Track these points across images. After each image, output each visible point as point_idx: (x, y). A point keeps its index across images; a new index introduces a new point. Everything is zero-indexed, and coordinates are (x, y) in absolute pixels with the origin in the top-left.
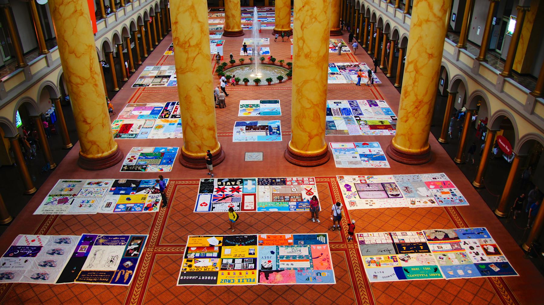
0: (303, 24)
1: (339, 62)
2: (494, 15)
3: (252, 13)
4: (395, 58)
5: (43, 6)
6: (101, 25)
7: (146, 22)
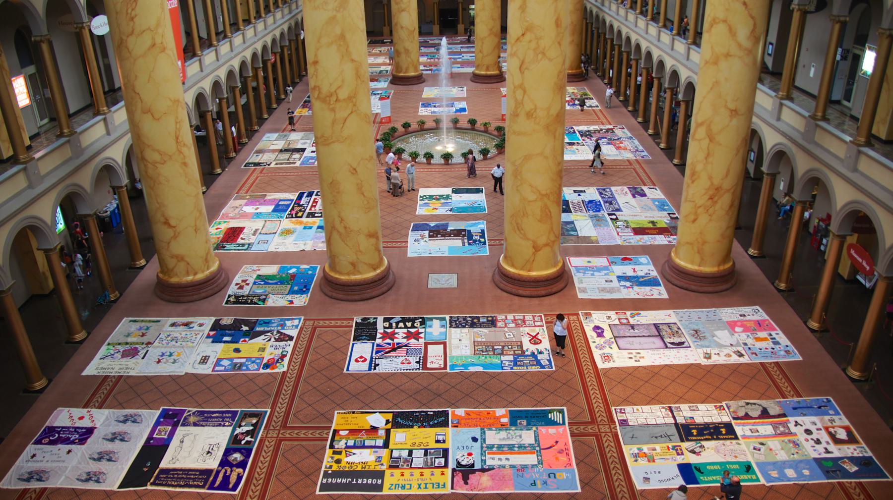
0: (523, 62)
3: (437, 46)
5: (102, 38)
6: (193, 68)
7: (265, 62)
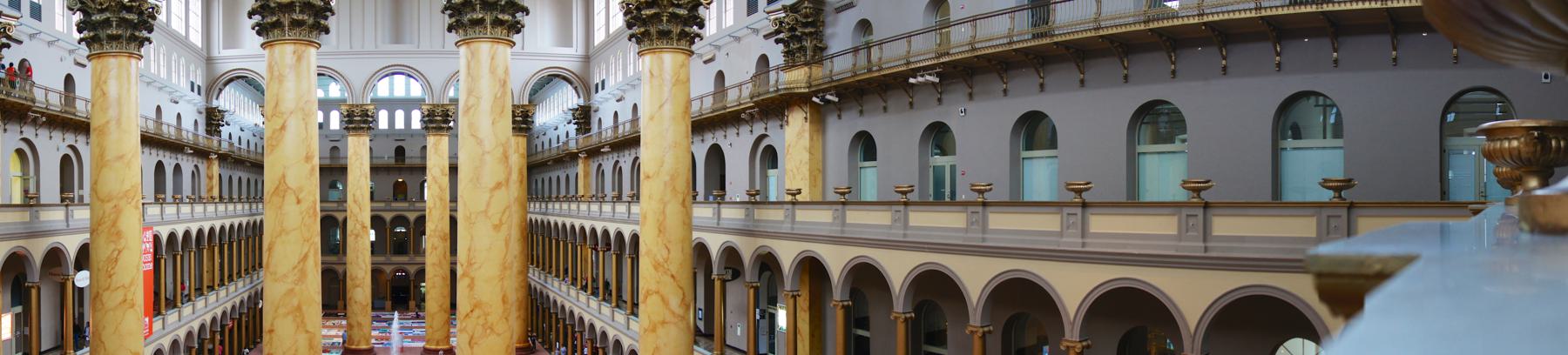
2: (756, 305)
5: (81, 290)
6: (157, 325)
7: (223, 327)
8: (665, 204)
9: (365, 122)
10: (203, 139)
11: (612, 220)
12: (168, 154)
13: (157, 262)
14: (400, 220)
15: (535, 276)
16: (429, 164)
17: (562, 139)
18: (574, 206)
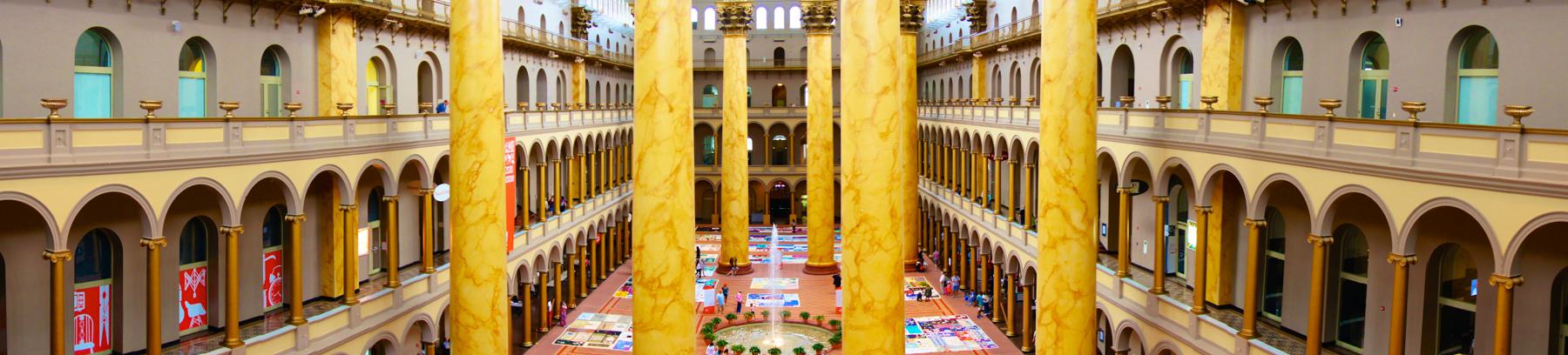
0: (858, 254)
1: (920, 315)
2: (1165, 221)
3: (768, 236)
4: (1018, 304)
5: (441, 204)
7: (589, 241)
8: (1067, 111)
9: (742, 21)
10: (569, 43)
11: (1010, 127)
12: (531, 59)
13: (519, 174)
14: (779, 128)
15: (926, 188)
16: (810, 66)
17: (956, 37)
18: (968, 111)
